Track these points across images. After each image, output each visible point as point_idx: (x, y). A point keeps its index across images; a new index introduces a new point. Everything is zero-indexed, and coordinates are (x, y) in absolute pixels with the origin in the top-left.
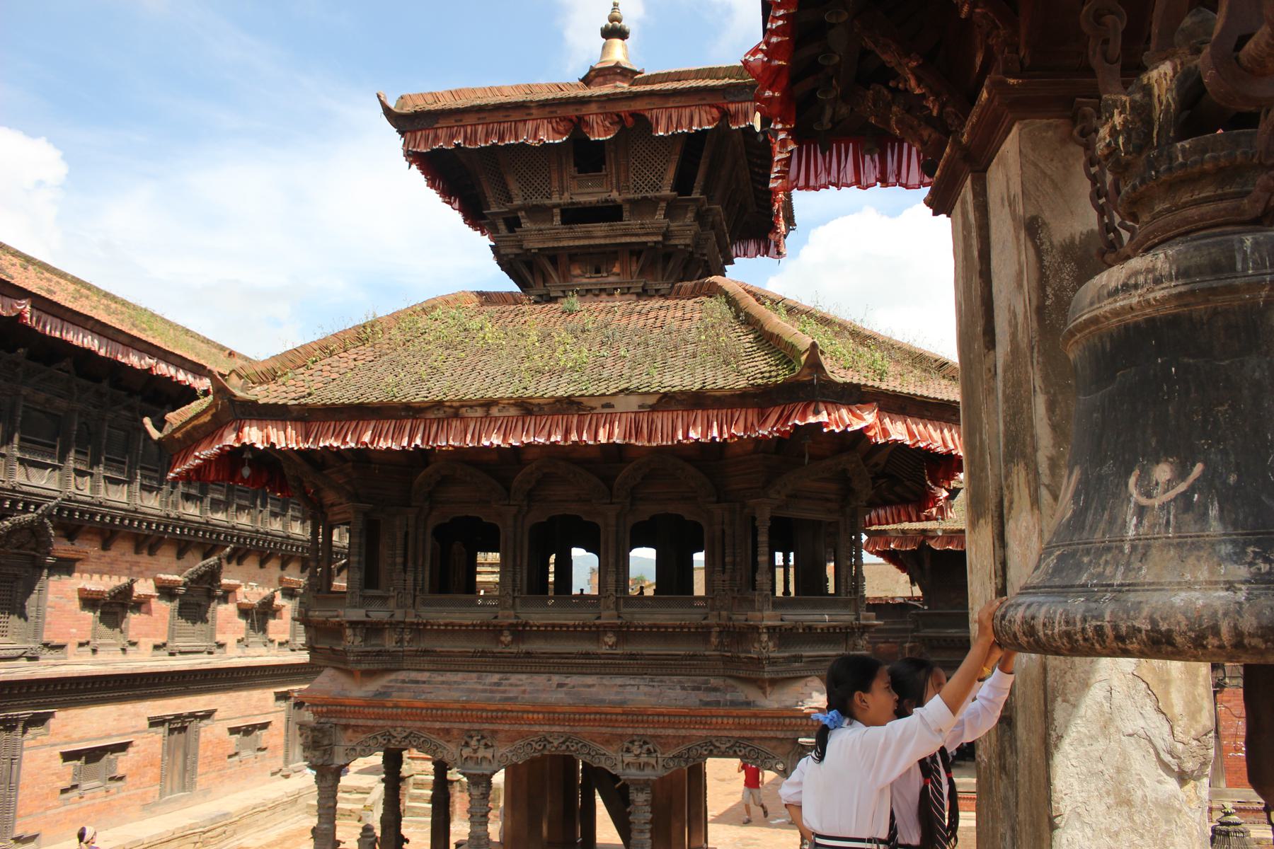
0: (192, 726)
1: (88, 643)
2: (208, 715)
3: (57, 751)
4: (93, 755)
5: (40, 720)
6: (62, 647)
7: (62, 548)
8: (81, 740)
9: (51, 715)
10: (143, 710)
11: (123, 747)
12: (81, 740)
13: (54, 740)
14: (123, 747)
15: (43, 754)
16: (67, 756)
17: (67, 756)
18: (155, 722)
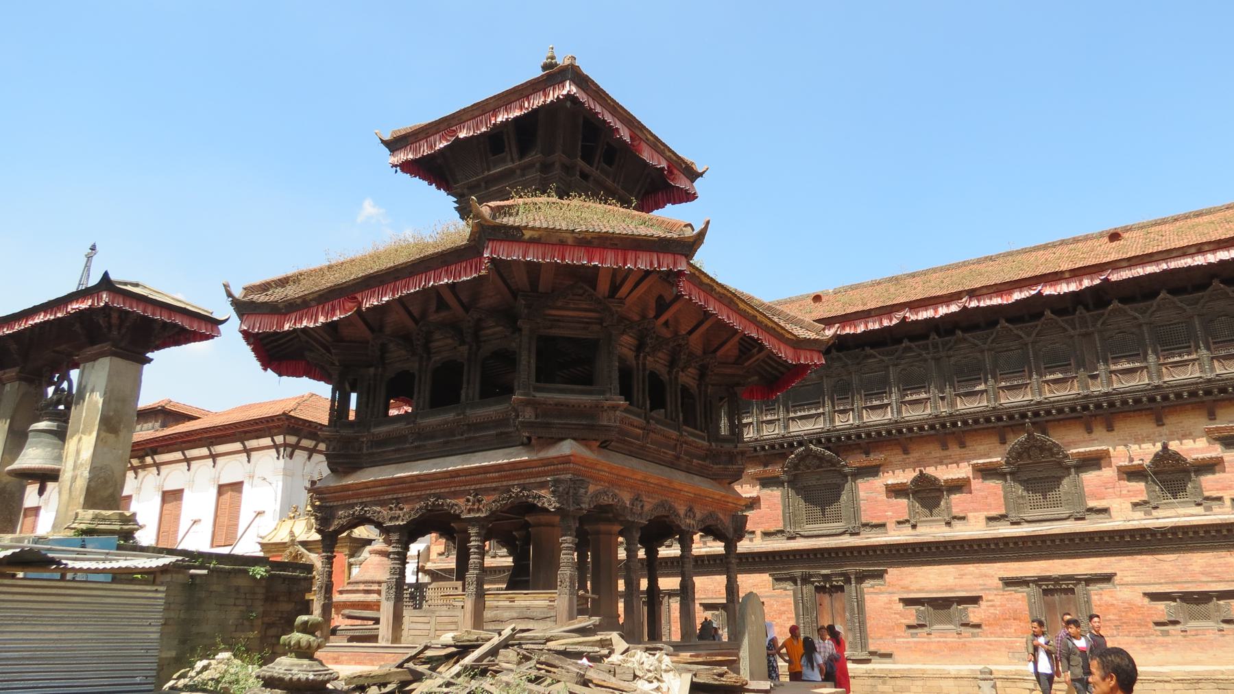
0: (1079, 589)
1: (908, 521)
2: (1107, 578)
3: (896, 598)
4: (941, 604)
5: (880, 575)
6: (883, 525)
7: (856, 461)
8: (920, 591)
9: (886, 571)
10: (991, 572)
11: (975, 600)
12: (920, 591)
13: (890, 590)
14: (975, 600)
15: (884, 598)
16: (908, 602)
17: (908, 602)
18: (1009, 582)
